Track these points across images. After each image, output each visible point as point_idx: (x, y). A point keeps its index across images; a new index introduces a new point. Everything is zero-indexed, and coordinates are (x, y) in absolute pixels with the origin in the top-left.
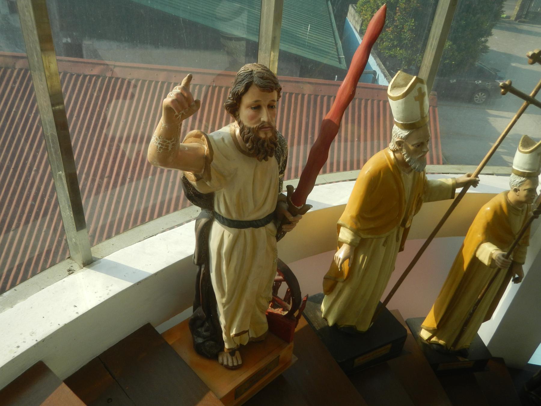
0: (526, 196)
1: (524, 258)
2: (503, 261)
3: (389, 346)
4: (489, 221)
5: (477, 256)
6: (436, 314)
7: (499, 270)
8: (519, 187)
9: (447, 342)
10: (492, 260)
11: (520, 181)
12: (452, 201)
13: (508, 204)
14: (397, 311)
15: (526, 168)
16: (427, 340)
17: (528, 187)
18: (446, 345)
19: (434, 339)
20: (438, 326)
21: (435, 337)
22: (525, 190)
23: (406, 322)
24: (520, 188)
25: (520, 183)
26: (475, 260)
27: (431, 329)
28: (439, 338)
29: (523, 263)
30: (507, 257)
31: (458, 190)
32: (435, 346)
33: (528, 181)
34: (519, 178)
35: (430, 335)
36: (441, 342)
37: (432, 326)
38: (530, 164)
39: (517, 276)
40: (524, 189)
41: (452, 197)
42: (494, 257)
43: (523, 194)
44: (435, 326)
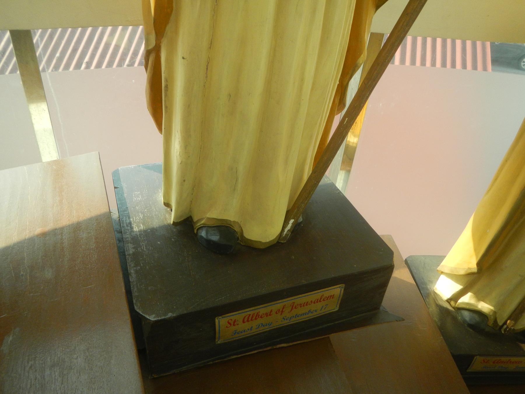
3: (337, 291)
6: (477, 237)
9: (500, 305)
14: (390, 238)
16: (449, 301)
18: (495, 313)
19: (467, 299)
20: (479, 264)
21: (469, 294)
23: (406, 262)
27: (462, 272)
28: (480, 297)
32: (467, 315)
35: (458, 287)
36: (485, 307)
37: (466, 266)
44: (473, 265)
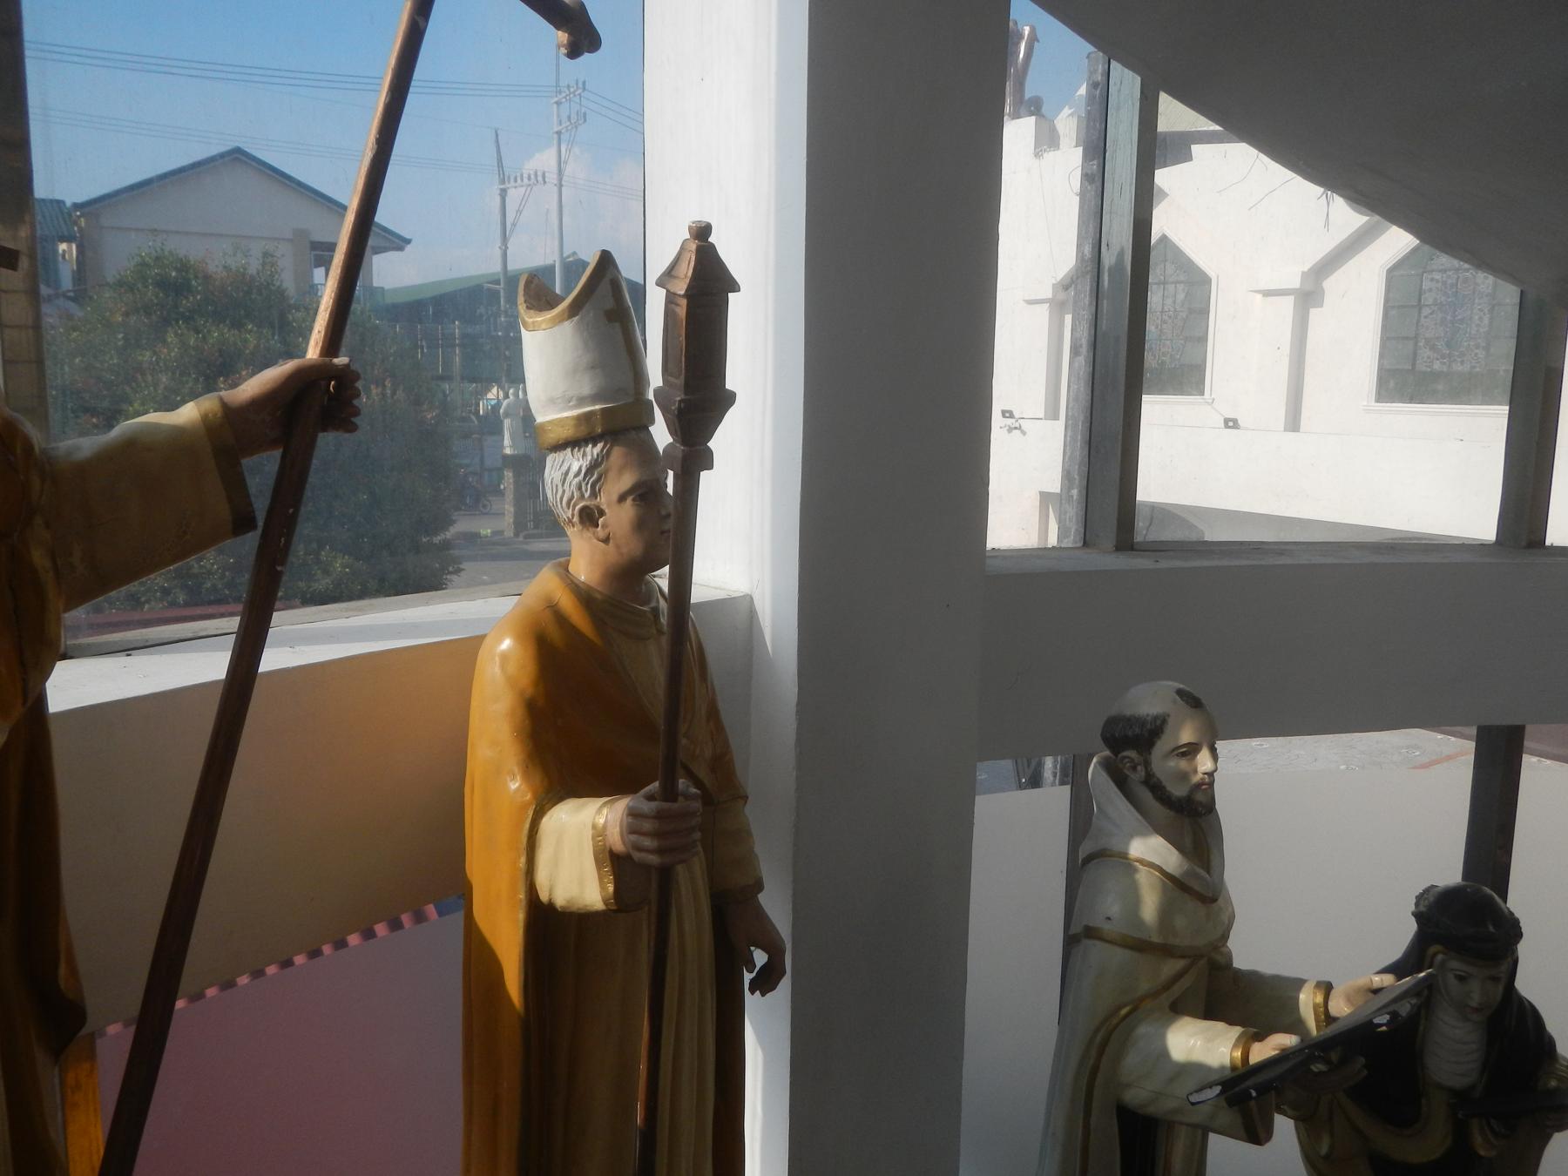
0: (640, 525)
1: (746, 861)
2: (659, 816)
4: (530, 691)
5: (544, 897)
7: (665, 876)
8: (594, 495)
10: (617, 864)
11: (585, 463)
12: (251, 540)
13: (585, 597)
15: (587, 389)
17: (627, 481)
22: (622, 498)
24: (603, 501)
25: (590, 471)
26: (546, 923)
29: (759, 886)
30: (669, 793)
31: (262, 470)
33: (617, 452)
34: (578, 453)
38: (592, 367)
39: (760, 958)
40: (615, 497)
41: (242, 523)
42: (616, 840)
43: (620, 517)
